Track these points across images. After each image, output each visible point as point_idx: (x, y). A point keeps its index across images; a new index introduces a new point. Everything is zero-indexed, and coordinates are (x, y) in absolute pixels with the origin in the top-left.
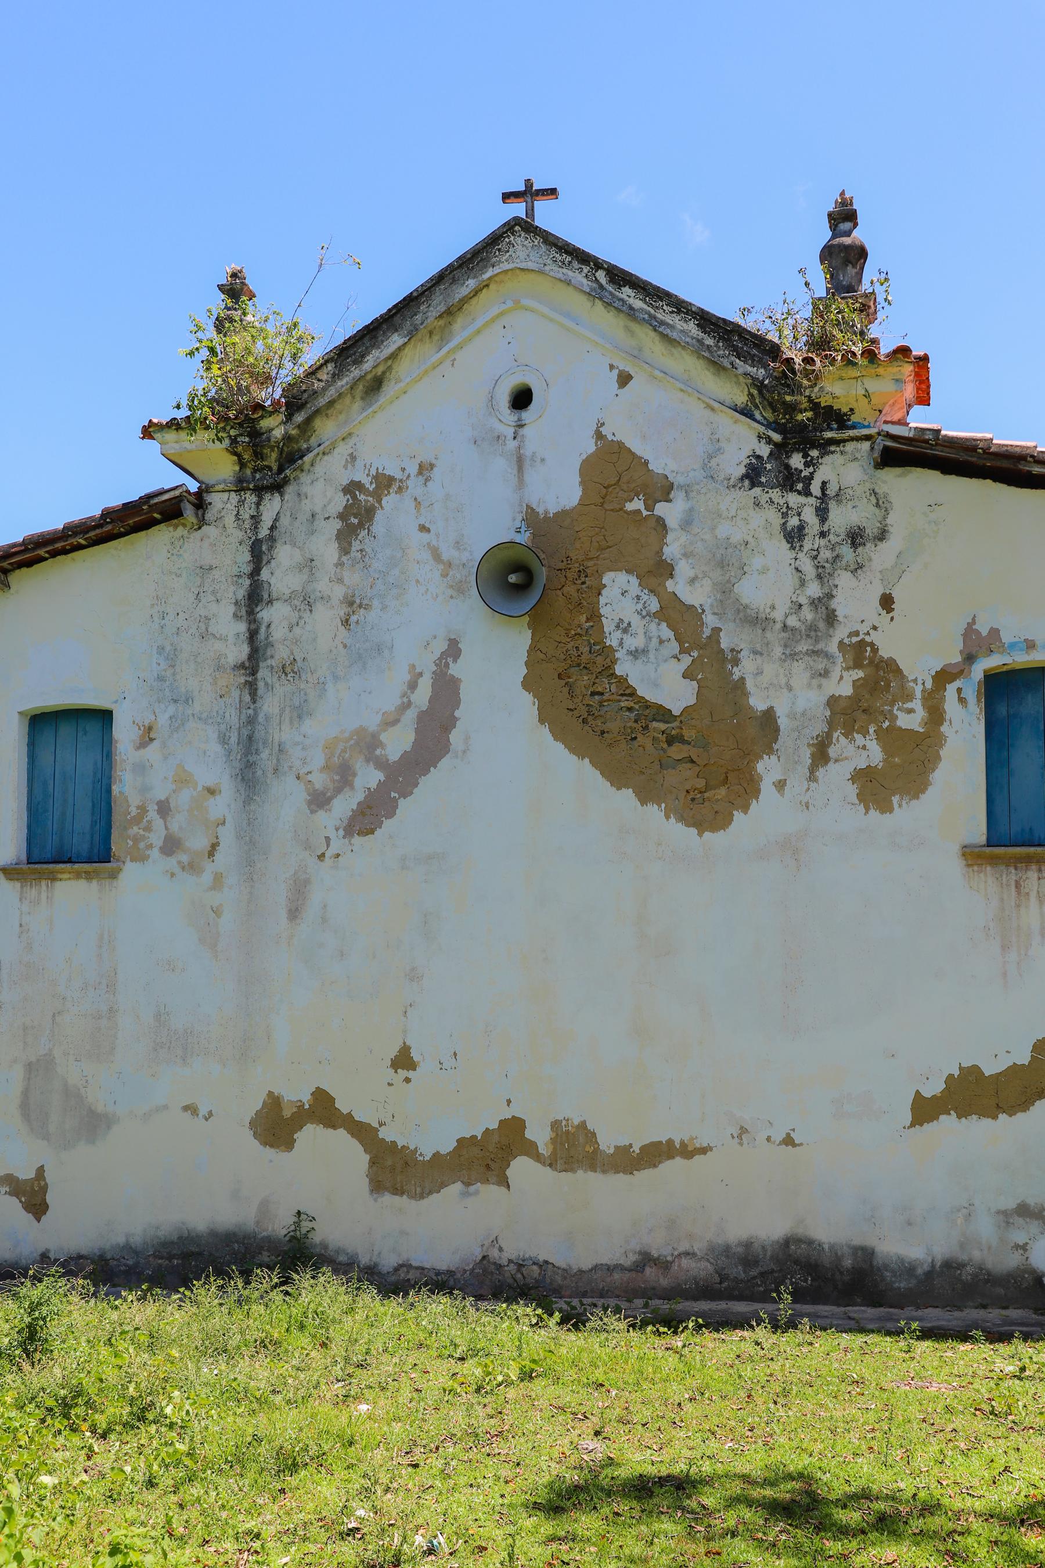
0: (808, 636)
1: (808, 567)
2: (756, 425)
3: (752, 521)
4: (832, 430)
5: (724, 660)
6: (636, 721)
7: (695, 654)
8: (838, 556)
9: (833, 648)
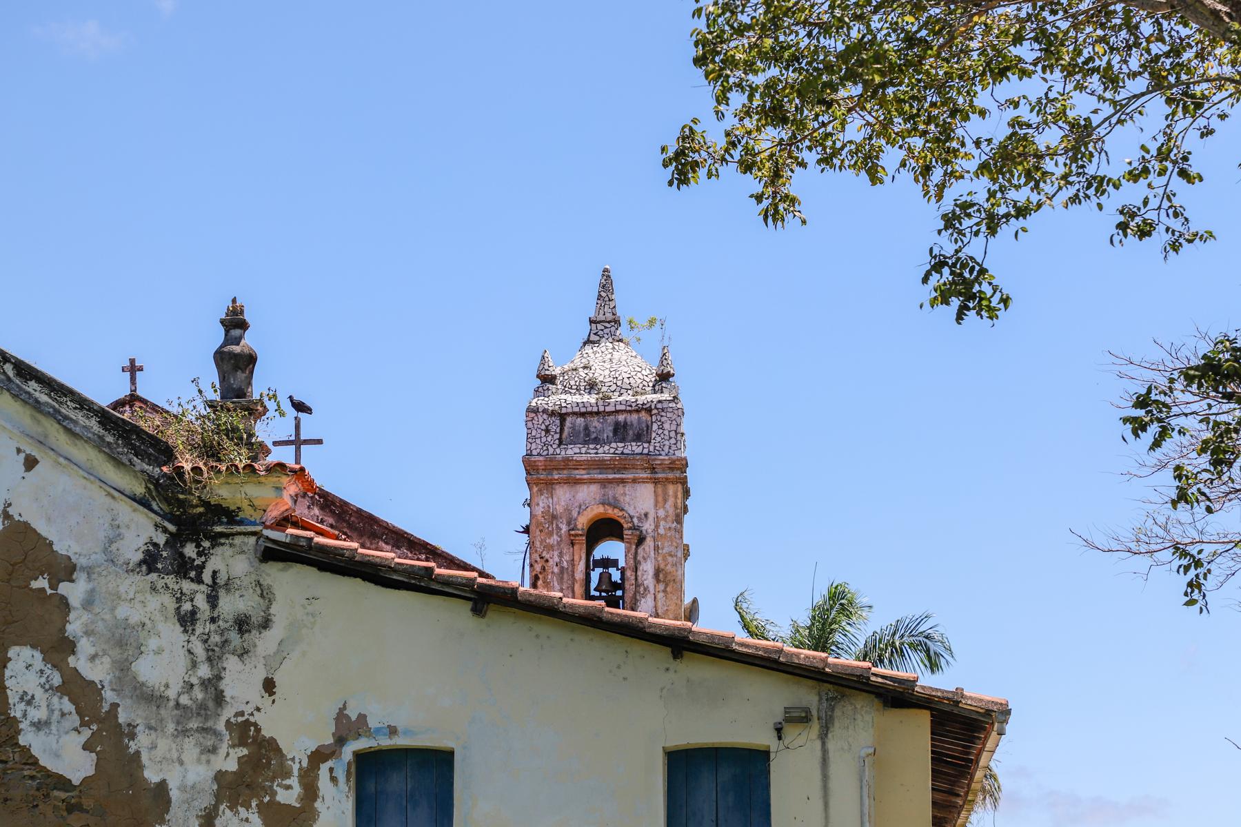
0: (198, 714)
1: (199, 649)
2: (153, 515)
3: (147, 603)
4: (221, 523)
5: (122, 734)
6: (38, 789)
7: (95, 727)
8: (226, 641)
9: (221, 726)
